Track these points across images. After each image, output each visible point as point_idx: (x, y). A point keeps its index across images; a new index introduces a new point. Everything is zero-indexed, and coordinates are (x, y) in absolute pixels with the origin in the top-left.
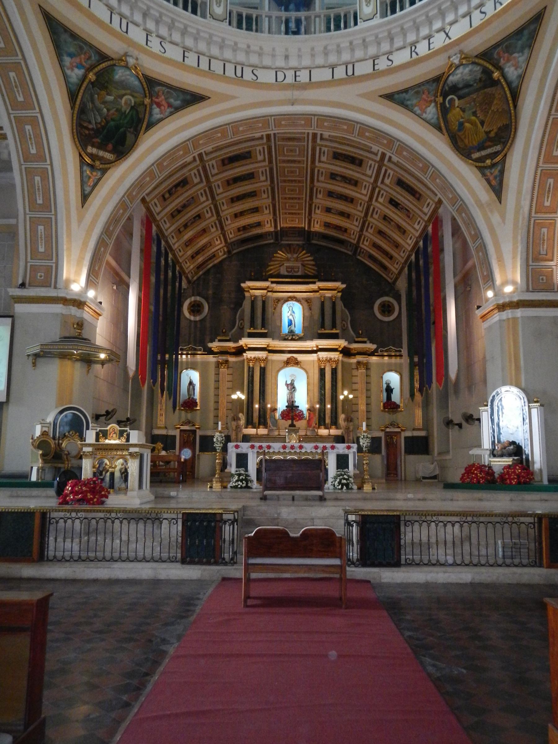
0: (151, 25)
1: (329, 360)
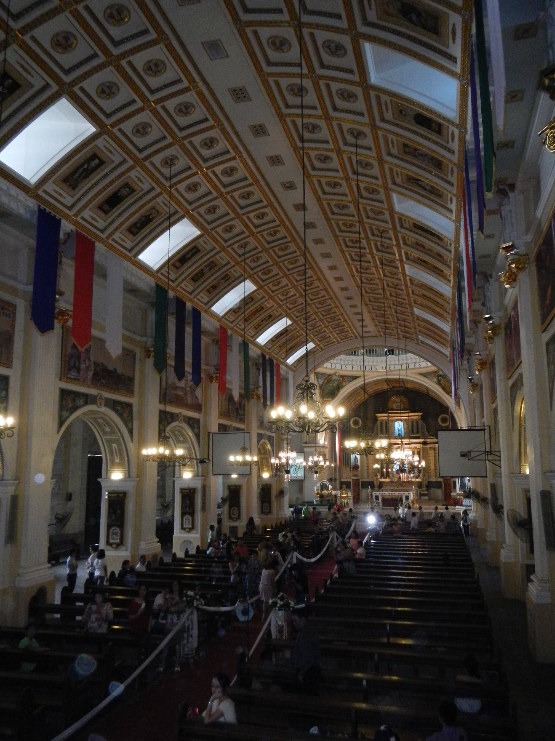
0: (342, 362)
1: (416, 448)
